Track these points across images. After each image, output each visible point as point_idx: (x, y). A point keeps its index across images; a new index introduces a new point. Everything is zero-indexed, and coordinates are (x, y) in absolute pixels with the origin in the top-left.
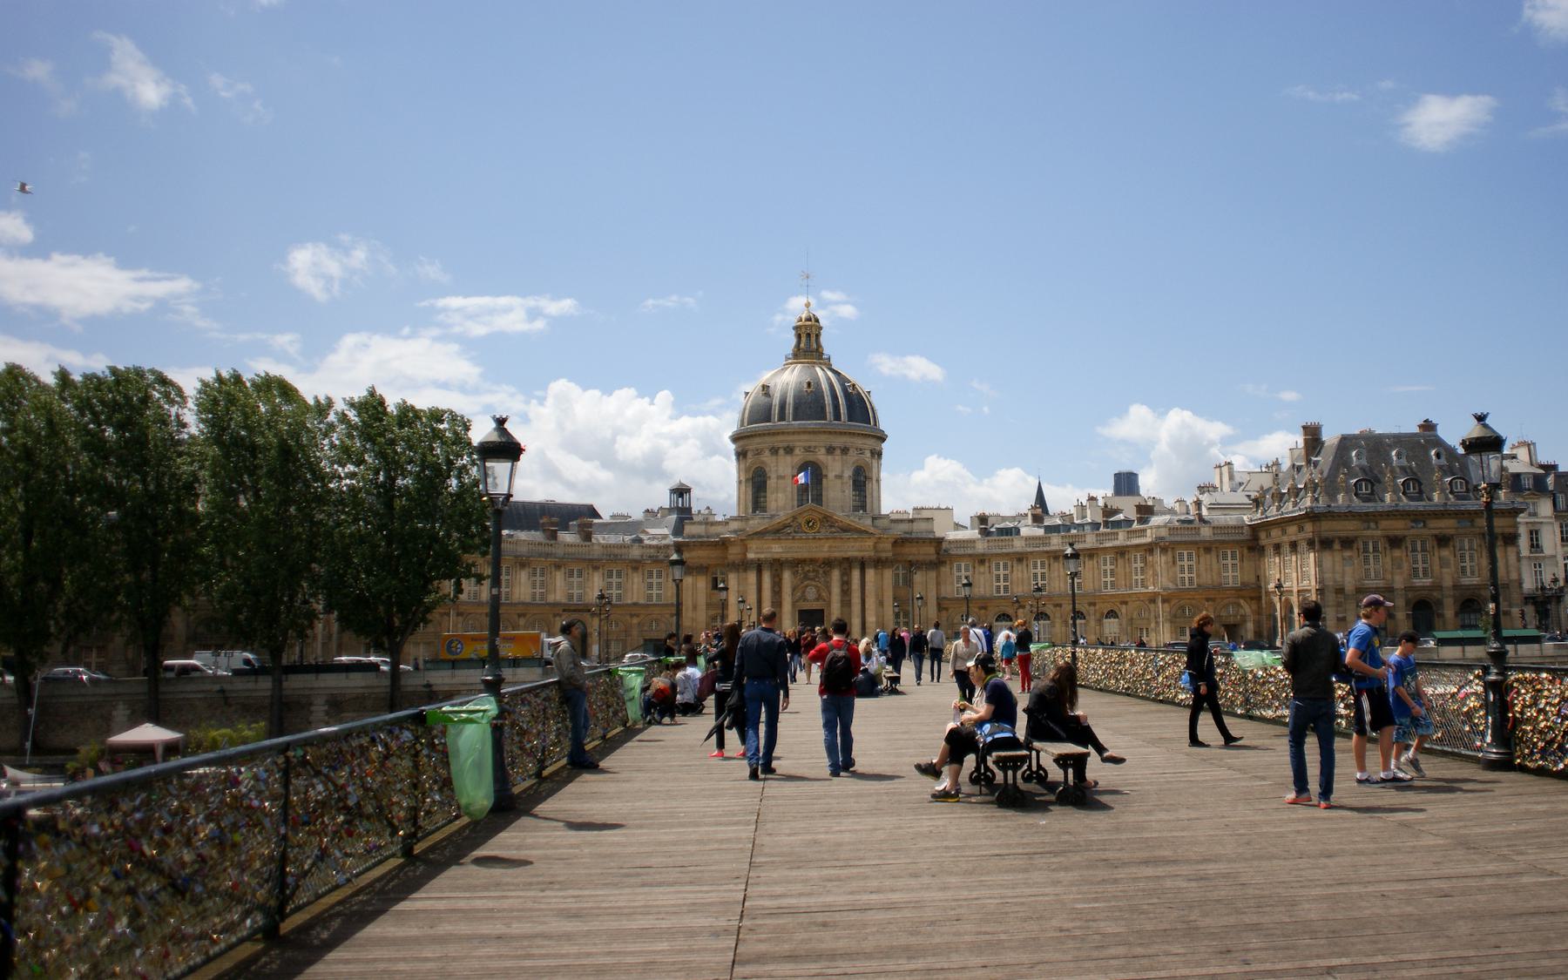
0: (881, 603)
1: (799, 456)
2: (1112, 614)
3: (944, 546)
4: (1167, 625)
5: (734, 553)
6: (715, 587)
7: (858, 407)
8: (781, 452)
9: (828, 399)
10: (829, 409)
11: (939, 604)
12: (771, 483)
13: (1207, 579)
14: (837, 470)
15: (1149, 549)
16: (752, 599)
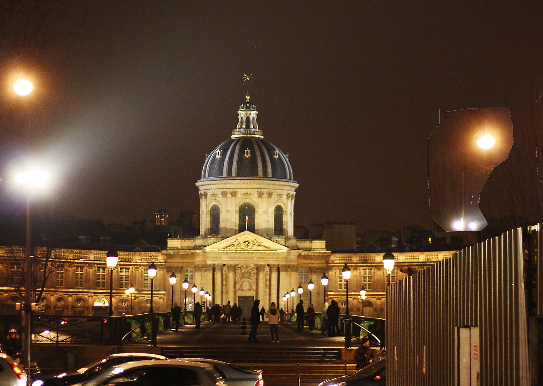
1: (240, 200)
8: (229, 195)
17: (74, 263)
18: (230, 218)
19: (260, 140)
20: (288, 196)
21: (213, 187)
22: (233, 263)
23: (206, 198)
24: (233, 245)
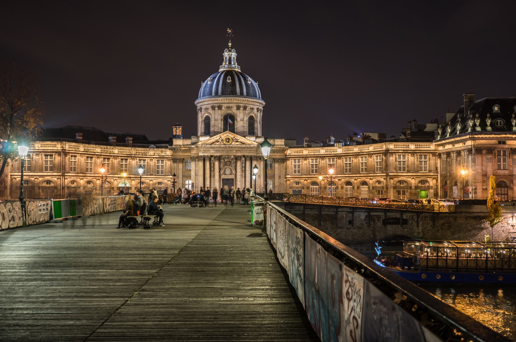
1: (224, 111)
4: (392, 189)
8: (216, 108)
16: (201, 173)
17: (101, 155)
18: (217, 123)
19: (239, 73)
20: (258, 109)
21: (206, 103)
22: (218, 154)
23: (201, 111)
24: (217, 141)
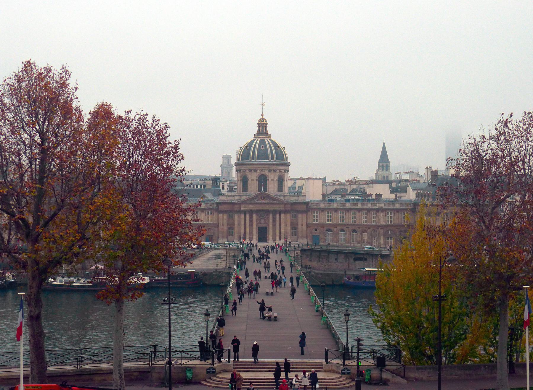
0: (286, 225)
1: (259, 173)
2: (365, 231)
3: (310, 205)
4: (382, 237)
5: (236, 207)
6: (229, 217)
7: (280, 154)
8: (253, 171)
9: (269, 152)
10: (270, 156)
11: (307, 225)
12: (249, 182)
13: (397, 222)
14: (272, 178)
15: (378, 210)
16: (243, 222)
